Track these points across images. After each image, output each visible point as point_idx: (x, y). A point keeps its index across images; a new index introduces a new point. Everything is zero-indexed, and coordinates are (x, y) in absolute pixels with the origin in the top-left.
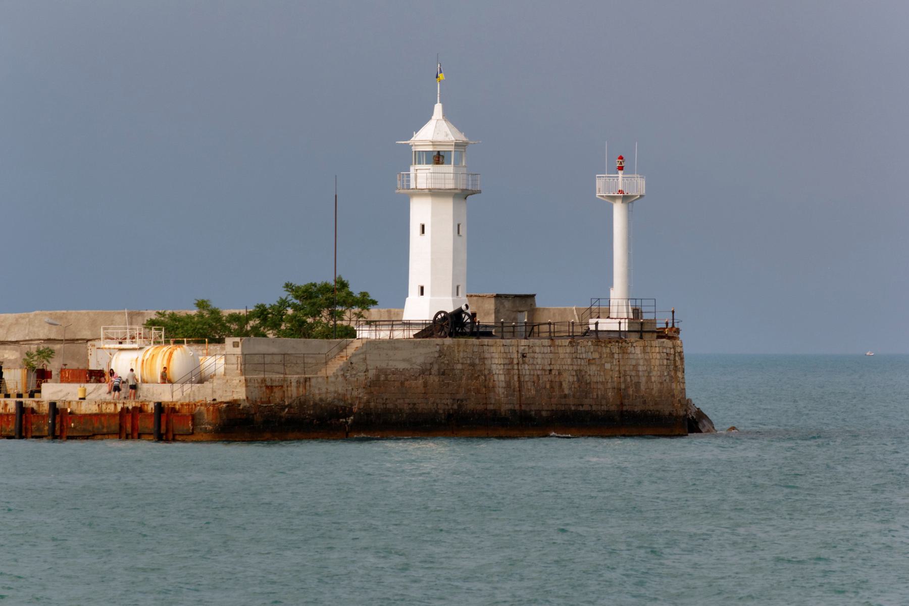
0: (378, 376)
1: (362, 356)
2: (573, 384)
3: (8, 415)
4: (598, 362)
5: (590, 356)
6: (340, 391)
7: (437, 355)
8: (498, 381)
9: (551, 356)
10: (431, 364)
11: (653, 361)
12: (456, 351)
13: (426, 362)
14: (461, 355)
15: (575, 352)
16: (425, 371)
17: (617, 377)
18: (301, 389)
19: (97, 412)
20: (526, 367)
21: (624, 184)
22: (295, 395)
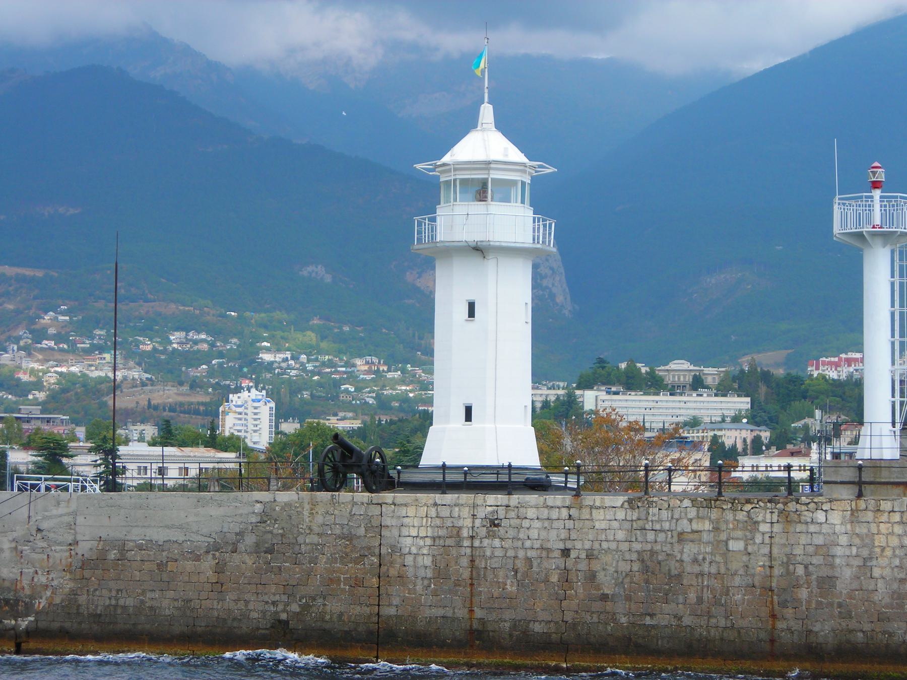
2: (627, 575)
4: (705, 537)
5: (684, 525)
7: (254, 519)
8: (415, 567)
9: (569, 524)
10: (241, 534)
11: (880, 541)
12: (306, 513)
13: (225, 530)
14: (319, 519)
15: (639, 519)
17: (763, 566)
20: (497, 542)
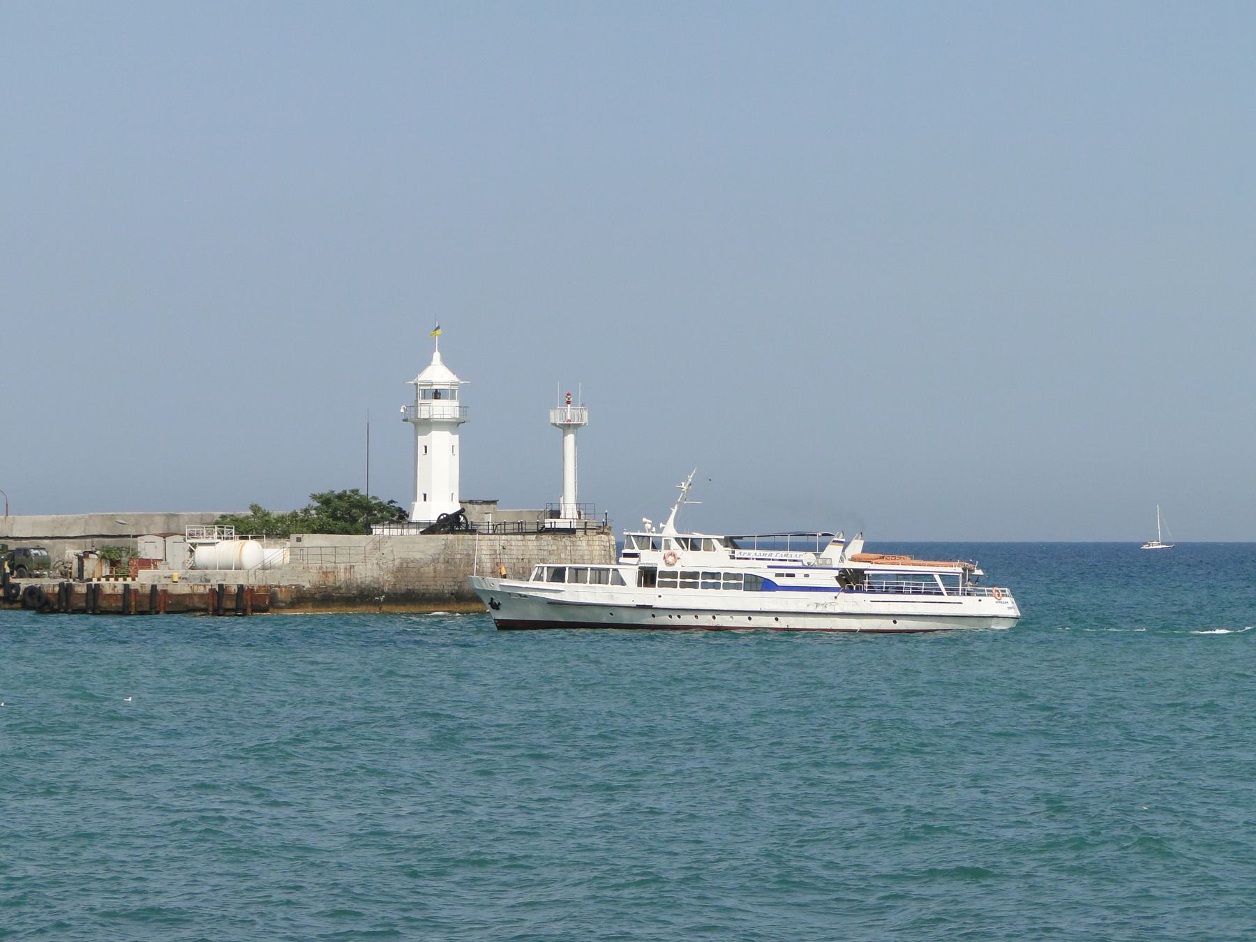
0: (402, 563)
1: (391, 548)
3: (117, 595)
5: (550, 548)
6: (375, 576)
9: (523, 548)
16: (434, 561)
18: (347, 574)
19: (190, 592)
21: (572, 415)
22: (343, 580)
